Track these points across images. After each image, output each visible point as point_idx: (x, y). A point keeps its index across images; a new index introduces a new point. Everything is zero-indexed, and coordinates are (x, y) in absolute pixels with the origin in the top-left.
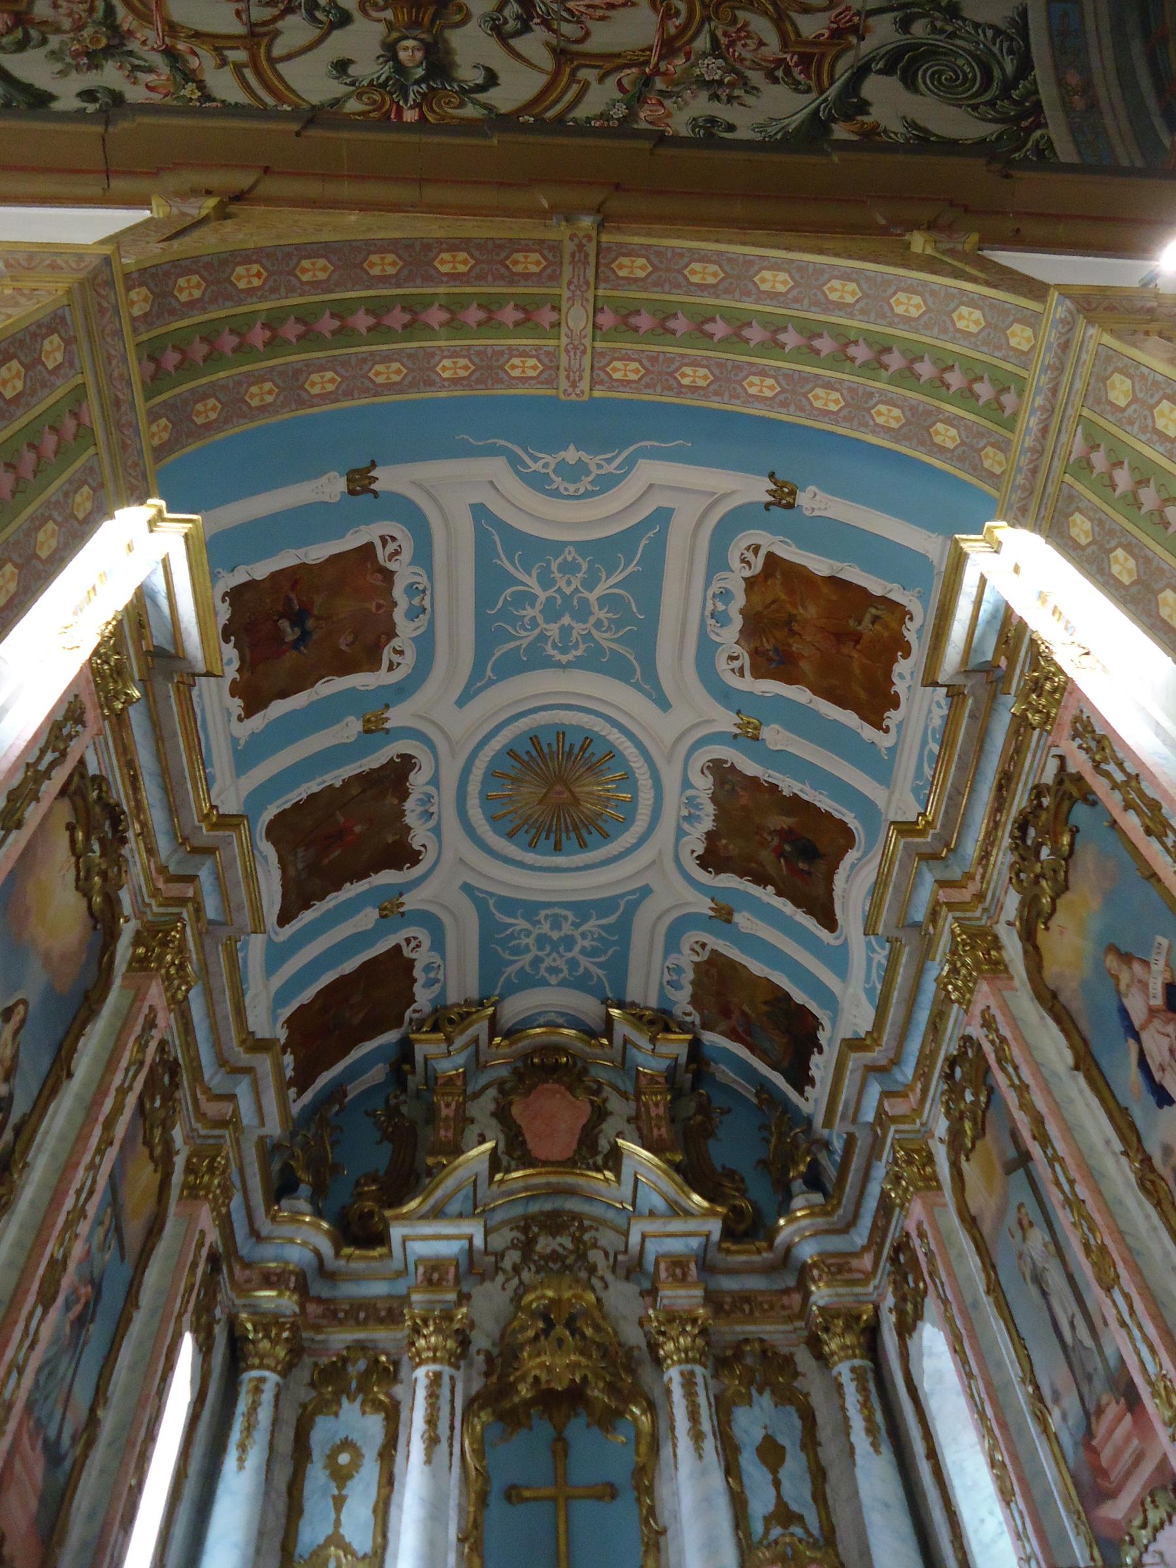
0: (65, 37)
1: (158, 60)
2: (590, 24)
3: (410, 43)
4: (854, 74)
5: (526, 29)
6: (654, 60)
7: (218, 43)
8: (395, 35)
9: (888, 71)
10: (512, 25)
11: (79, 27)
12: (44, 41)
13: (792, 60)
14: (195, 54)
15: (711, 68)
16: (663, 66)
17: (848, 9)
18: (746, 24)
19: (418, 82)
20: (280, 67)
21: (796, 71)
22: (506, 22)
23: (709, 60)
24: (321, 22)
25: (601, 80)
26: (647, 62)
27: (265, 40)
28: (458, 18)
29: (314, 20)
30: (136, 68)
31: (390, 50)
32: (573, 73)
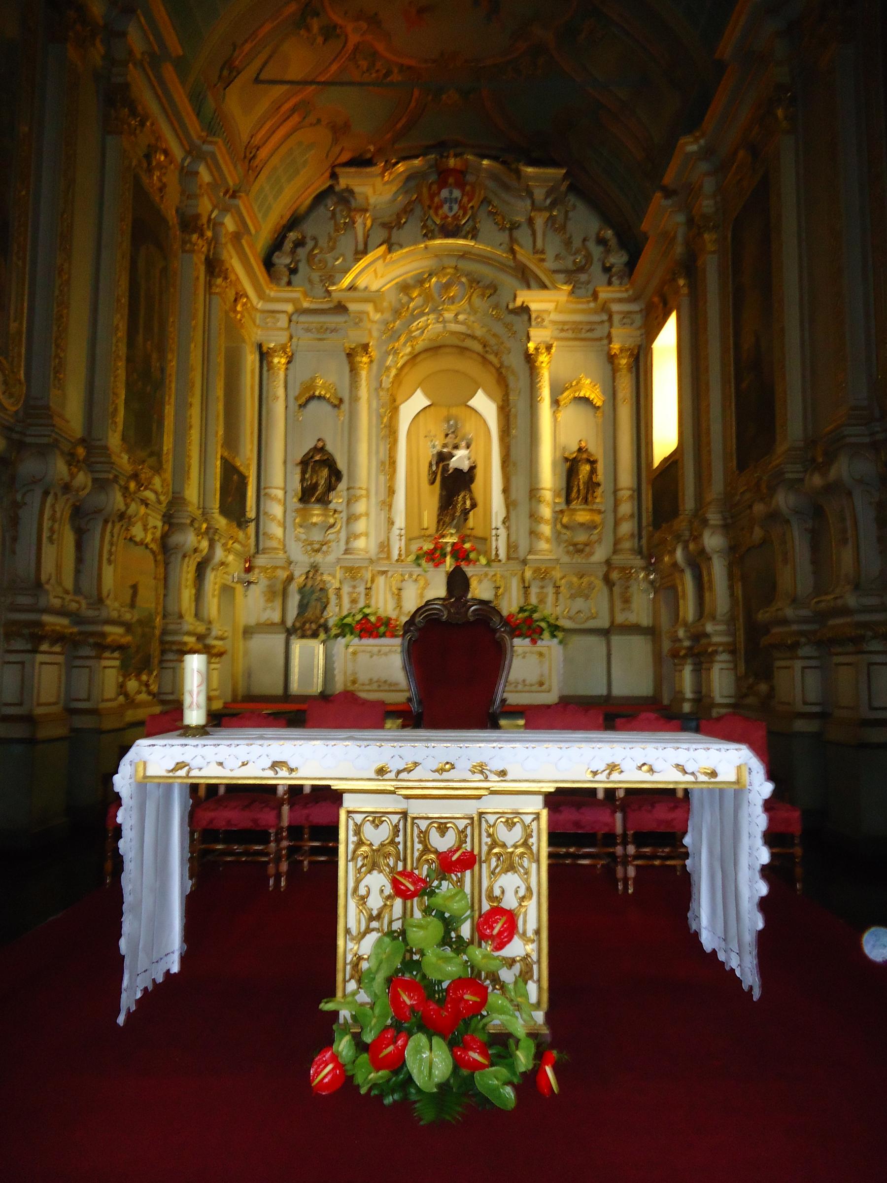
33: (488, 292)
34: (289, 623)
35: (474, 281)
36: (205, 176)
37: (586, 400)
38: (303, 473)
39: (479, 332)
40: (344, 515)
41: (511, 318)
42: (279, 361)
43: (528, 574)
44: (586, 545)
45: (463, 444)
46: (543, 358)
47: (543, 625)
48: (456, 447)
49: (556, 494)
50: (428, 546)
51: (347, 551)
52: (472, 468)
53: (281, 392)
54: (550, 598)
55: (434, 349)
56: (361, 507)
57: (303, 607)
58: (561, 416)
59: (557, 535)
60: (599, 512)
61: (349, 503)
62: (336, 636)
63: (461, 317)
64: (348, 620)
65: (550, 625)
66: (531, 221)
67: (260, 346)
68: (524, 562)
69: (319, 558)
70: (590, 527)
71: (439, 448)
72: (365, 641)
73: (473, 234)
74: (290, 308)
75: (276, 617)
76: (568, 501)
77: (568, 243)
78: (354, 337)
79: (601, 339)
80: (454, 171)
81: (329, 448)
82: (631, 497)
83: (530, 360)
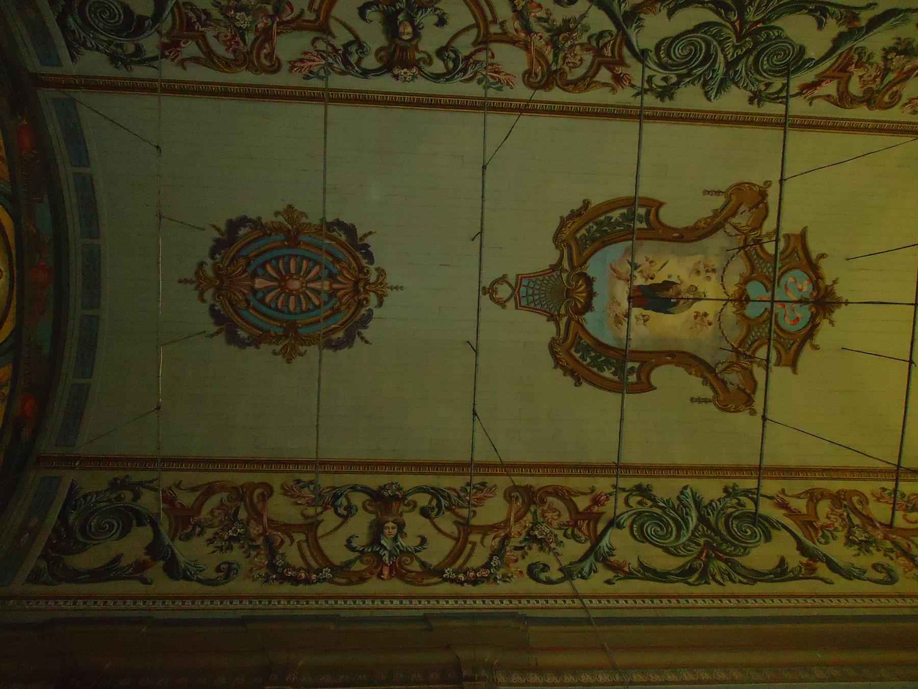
0: (580, 41)
1: (536, 26)
2: (311, 49)
3: (406, 37)
4: (161, 15)
5: (346, 46)
6: (275, 26)
7: (505, 38)
8: (414, 42)
9: (142, 19)
11: (572, 46)
12: (590, 38)
14: (516, 30)
15: (243, 19)
16: (269, 22)
17: (173, 60)
18: (227, 50)
19: (401, 10)
20: (473, 22)
21: (194, 20)
22: (357, 51)
23: (244, 26)
24: (451, 50)
25: (302, 12)
26: (279, 24)
27: (480, 40)
28: (382, 53)
29: (455, 52)
30: (546, 20)
31: (416, 34)
32: (318, 16)
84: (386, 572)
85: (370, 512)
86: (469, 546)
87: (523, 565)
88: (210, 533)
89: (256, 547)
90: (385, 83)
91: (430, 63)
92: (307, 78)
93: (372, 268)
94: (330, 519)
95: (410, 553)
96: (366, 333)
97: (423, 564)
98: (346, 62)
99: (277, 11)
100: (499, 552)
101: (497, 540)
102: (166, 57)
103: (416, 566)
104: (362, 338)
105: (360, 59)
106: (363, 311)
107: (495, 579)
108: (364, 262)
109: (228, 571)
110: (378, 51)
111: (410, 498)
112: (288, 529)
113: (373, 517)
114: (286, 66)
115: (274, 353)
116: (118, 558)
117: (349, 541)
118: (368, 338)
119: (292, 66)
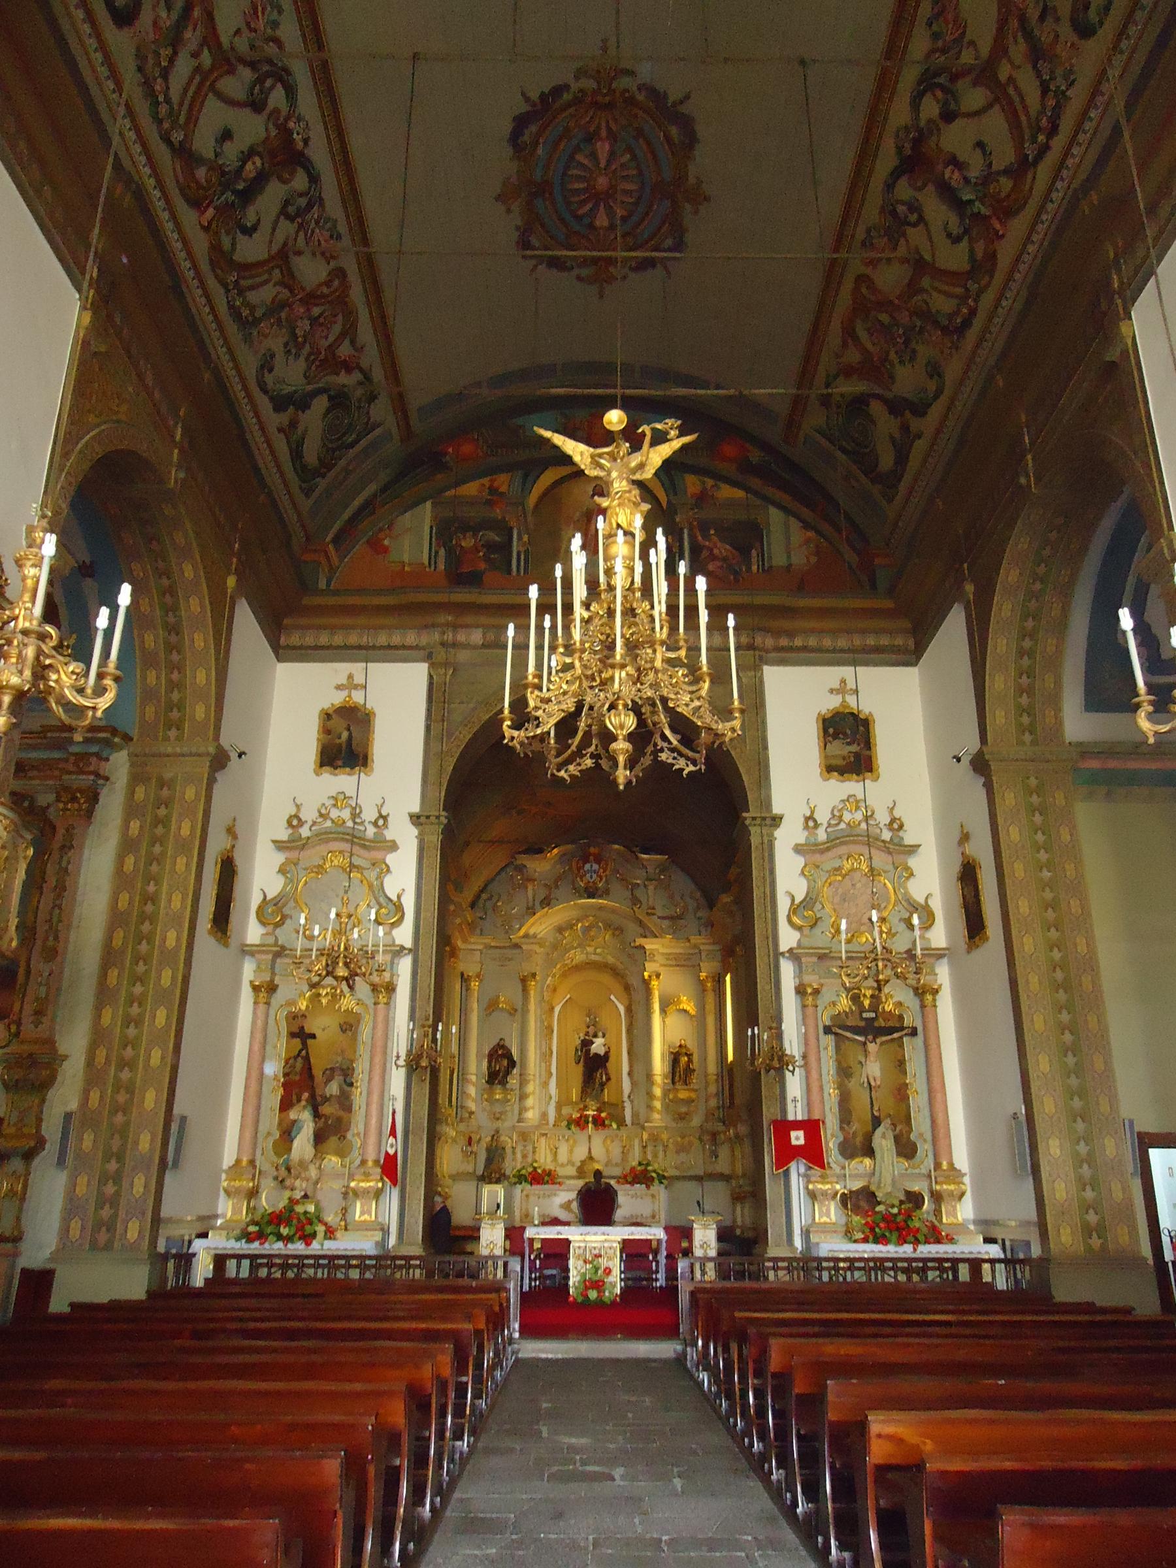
5: (291, 219)
7: (211, 38)
8: (260, 149)
9: (330, 398)
10: (291, 210)
13: (322, 357)
18: (335, 323)
19: (234, 192)
23: (307, 322)
32: (273, 268)
33: (617, 933)
34: (480, 1172)
35: (608, 926)
36: (452, 908)
37: (685, 1011)
38: (490, 1062)
39: (611, 960)
40: (517, 1092)
41: (635, 950)
42: (475, 985)
43: (645, 1136)
44: (687, 1114)
45: (600, 1034)
46: (654, 983)
47: (654, 1175)
48: (595, 1036)
49: (665, 1076)
50: (576, 1115)
51: (519, 1121)
52: (607, 1054)
53: (475, 1006)
54: (661, 1154)
55: (578, 968)
56: (530, 1088)
57: (489, 1161)
58: (668, 1020)
59: (666, 1107)
60: (696, 1091)
61: (521, 1084)
62: (515, 1184)
63: (599, 951)
64: (523, 1172)
65: (658, 1174)
66: (645, 886)
67: (462, 974)
68: (643, 1128)
69: (499, 1124)
70: (689, 1101)
71: (582, 1037)
72: (534, 1187)
73: (605, 893)
74: (480, 947)
75: (470, 1169)
76: (673, 1083)
77: (671, 897)
78: (527, 968)
79: (694, 966)
80: (594, 855)
81: (507, 1044)
82: (717, 1080)
83: (646, 983)
84: (998, 226)
85: (925, 185)
86: (1011, 91)
87: (1066, 30)
88: (892, 356)
89: (922, 331)
90: (319, 154)
91: (276, 111)
92: (339, 237)
93: (575, 86)
94: (915, 235)
95: (988, 178)
96: (674, 96)
97: (1006, 172)
98: (310, 206)
99: (283, 305)
100: (1037, 54)
101: (1021, 40)
102: (358, 364)
103: (1006, 184)
104: (681, 102)
105: (301, 195)
106: (640, 97)
107: (1063, 93)
108: (566, 97)
109: (934, 371)
110: (285, 182)
111: (922, 123)
112: (913, 288)
113: (931, 188)
114: (333, 264)
115: (696, 212)
116: (893, 439)
117: (949, 235)
118: (680, 96)
119: (328, 257)
